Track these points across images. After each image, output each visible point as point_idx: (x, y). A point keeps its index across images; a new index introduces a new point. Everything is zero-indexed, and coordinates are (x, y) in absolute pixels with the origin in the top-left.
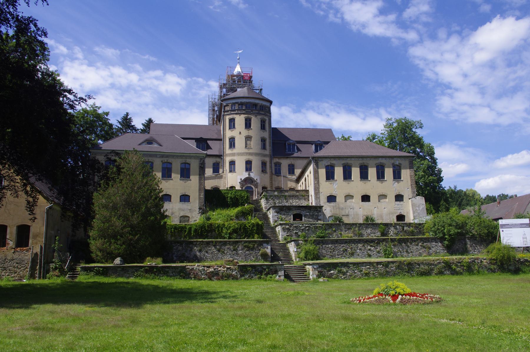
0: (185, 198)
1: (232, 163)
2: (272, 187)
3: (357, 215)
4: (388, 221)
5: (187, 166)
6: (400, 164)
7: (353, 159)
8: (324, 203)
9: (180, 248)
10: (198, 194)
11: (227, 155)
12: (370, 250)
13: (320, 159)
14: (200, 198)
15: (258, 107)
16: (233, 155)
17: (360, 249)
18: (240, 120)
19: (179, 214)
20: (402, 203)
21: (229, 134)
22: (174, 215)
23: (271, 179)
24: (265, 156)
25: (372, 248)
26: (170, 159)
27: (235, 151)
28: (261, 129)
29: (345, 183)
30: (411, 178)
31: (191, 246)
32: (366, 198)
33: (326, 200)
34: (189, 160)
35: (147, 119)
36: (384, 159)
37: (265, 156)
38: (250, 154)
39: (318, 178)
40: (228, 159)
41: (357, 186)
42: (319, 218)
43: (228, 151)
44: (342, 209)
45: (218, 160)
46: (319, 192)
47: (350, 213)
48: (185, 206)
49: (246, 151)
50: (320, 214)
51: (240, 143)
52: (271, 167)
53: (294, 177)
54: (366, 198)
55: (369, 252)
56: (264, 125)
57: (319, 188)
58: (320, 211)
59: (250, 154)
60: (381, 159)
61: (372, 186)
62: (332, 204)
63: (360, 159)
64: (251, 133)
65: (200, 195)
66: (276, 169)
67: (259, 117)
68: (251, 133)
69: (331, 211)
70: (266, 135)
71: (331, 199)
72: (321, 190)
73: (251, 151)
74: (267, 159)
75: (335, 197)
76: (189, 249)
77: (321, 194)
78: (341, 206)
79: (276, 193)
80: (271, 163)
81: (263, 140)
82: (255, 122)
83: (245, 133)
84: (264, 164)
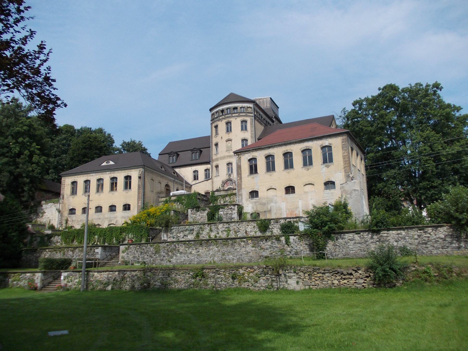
0: (127, 207)
3: (280, 209)
6: (330, 144)
8: (247, 200)
11: (213, 161)
15: (239, 108)
16: (217, 159)
18: (222, 125)
20: (332, 191)
21: (214, 141)
27: (219, 156)
28: (242, 129)
30: (344, 158)
32: (290, 190)
33: (248, 197)
39: (241, 174)
40: (214, 164)
41: (281, 177)
42: (233, 216)
43: (214, 157)
44: (264, 204)
45: (208, 166)
46: (241, 189)
47: (272, 208)
50: (234, 212)
54: (290, 190)
55: (190, 256)
56: (246, 127)
61: (298, 175)
62: (255, 199)
65: (138, 203)
67: (239, 119)
68: (231, 136)
69: (253, 208)
71: (254, 194)
72: (243, 186)
75: (258, 192)
78: (264, 201)
82: (236, 123)
83: (226, 137)
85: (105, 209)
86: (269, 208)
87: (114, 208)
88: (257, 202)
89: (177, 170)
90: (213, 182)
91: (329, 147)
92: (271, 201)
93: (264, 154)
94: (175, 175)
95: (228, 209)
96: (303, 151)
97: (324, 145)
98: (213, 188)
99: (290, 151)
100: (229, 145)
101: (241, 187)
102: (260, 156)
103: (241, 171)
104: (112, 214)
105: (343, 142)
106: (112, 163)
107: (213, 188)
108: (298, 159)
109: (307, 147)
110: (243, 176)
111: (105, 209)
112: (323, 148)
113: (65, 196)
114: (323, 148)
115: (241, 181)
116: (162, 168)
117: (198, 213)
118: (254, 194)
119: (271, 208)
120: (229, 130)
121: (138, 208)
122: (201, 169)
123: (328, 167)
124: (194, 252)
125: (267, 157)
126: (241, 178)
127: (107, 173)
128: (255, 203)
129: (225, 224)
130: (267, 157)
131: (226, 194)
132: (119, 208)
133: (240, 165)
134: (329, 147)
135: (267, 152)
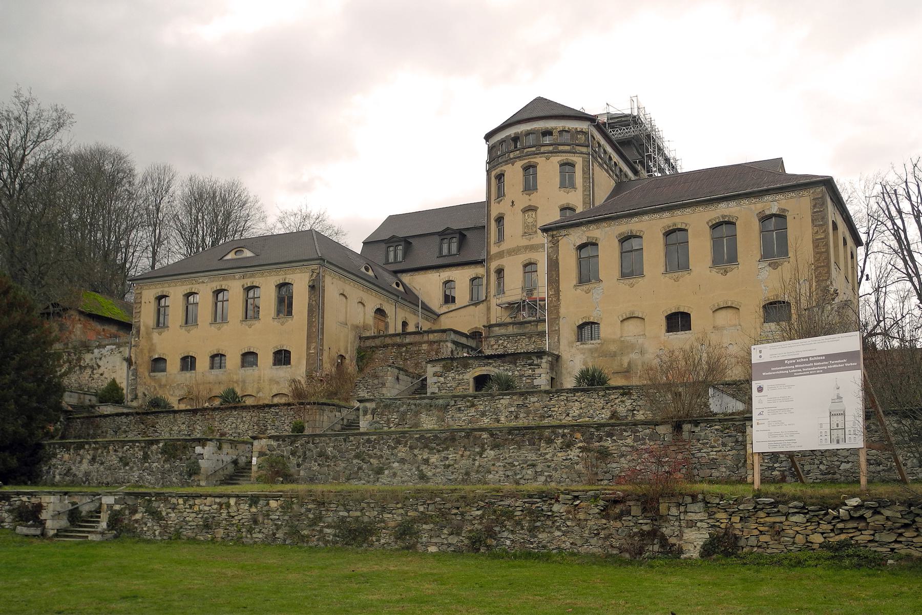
0: (282, 357)
6: (784, 210)
7: (646, 218)
8: (570, 345)
9: (66, 456)
12: (426, 461)
13: (563, 232)
17: (402, 461)
19: (271, 389)
25: (434, 459)
26: (257, 280)
29: (624, 286)
31: (81, 452)
32: (678, 321)
33: (573, 337)
36: (732, 204)
41: (657, 291)
42: (536, 382)
44: (614, 355)
46: (558, 318)
50: (537, 371)
54: (678, 321)
55: (423, 467)
57: (557, 307)
58: (539, 366)
60: (723, 205)
63: (667, 214)
65: (308, 348)
69: (585, 363)
72: (563, 311)
76: (78, 459)
77: (562, 322)
78: (613, 348)
85: (233, 360)
86: (626, 365)
87: (250, 358)
88: (596, 350)
89: (406, 278)
91: (781, 216)
92: (632, 347)
93: (617, 233)
94: (401, 288)
95: (524, 366)
96: (715, 227)
97: (768, 213)
98: (488, 319)
99: (683, 227)
101: (558, 313)
102: (607, 237)
103: (558, 276)
105: (815, 206)
107: (488, 319)
108: (700, 247)
109: (723, 216)
110: (563, 286)
111: (233, 360)
112: (765, 218)
113: (142, 329)
114: (765, 218)
115: (558, 299)
116: (367, 269)
117: (451, 375)
118: (586, 329)
119: (629, 364)
121: (308, 360)
123: (774, 266)
124: (434, 459)
125: (625, 239)
126: (557, 292)
127: (237, 276)
128: (591, 351)
129: (515, 398)
130: (625, 239)
131: (521, 331)
132: (266, 358)
133: (557, 259)
134: (781, 216)
135: (624, 227)
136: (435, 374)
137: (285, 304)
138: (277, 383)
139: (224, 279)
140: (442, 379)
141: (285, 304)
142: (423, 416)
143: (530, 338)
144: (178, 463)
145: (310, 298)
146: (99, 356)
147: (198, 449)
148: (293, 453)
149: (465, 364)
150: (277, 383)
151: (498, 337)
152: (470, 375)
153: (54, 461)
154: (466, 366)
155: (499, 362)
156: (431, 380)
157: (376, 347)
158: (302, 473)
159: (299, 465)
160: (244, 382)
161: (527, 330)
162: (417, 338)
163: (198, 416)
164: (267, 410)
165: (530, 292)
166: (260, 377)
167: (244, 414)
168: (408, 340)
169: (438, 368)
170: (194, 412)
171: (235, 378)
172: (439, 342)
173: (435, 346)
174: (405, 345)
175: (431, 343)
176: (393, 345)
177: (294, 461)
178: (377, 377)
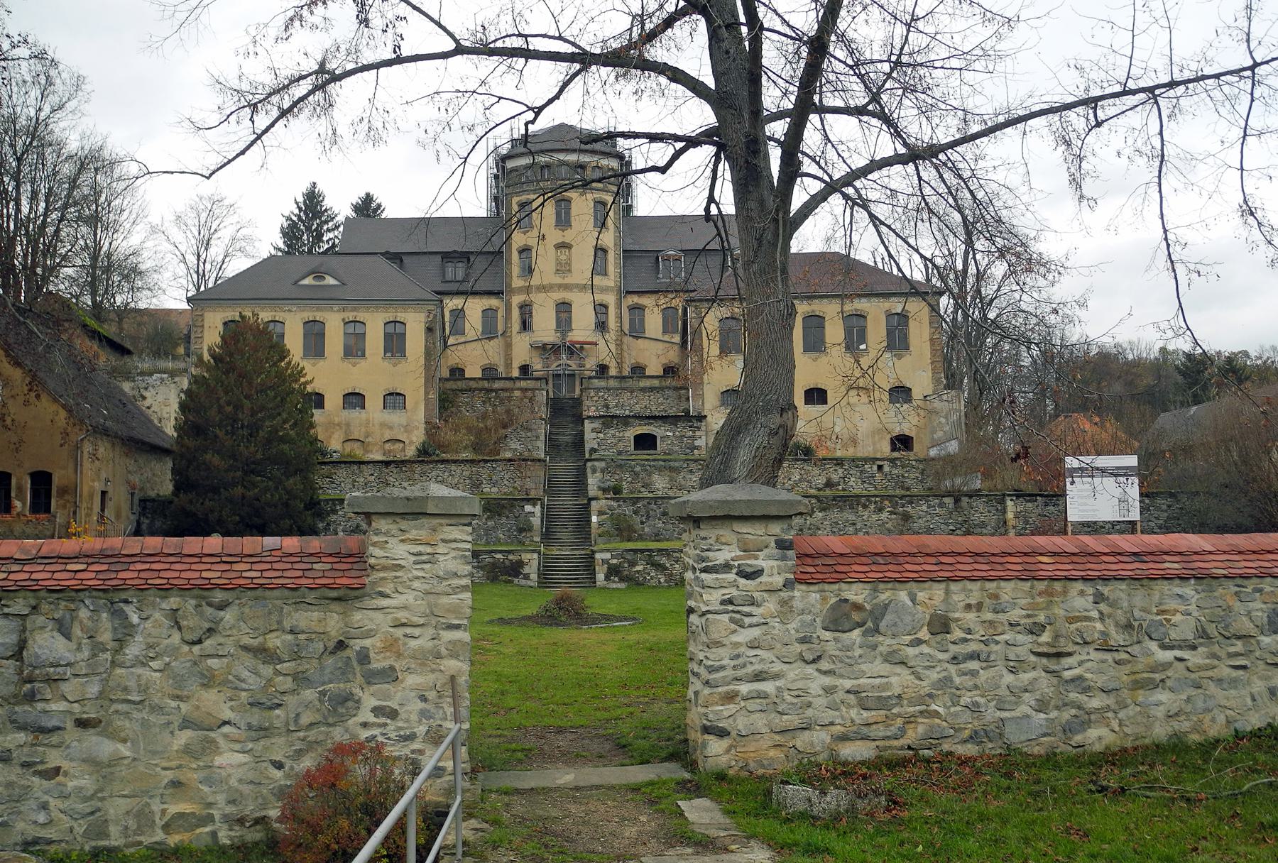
0: (394, 399)
1: (526, 309)
2: (620, 365)
4: (864, 451)
5: (399, 328)
10: (422, 390)
11: (512, 291)
14: (426, 399)
19: (382, 435)
22: (370, 439)
23: (619, 345)
24: (604, 290)
33: (718, 403)
34: (403, 315)
35: (363, 195)
37: (604, 290)
38: (566, 287)
40: (516, 300)
42: (696, 443)
43: (517, 282)
45: (494, 302)
48: (396, 418)
49: (558, 280)
50: (698, 433)
51: (545, 263)
52: (620, 317)
53: (677, 339)
59: (566, 287)
64: (568, 236)
65: (426, 393)
66: (632, 321)
68: (568, 236)
70: (608, 239)
73: (568, 281)
74: (610, 299)
79: (612, 383)
80: (619, 306)
81: (600, 251)
83: (554, 236)
84: (601, 308)
87: (354, 400)
90: (508, 346)
100: (563, 257)
104: (355, 415)
106: (330, 281)
111: (333, 401)
120: (563, 221)
122: (475, 308)
132: (374, 402)
136: (593, 430)
137: (395, 343)
138: (391, 428)
139: (318, 310)
140: (601, 435)
141: (395, 343)
142: (655, 477)
143: (632, 393)
144: (504, 520)
145: (426, 340)
146: (144, 385)
147: (528, 508)
148: (636, 512)
149: (625, 421)
150: (391, 428)
151: (598, 389)
152: (631, 433)
153: (333, 518)
154: (626, 424)
155: (660, 423)
156: (589, 435)
157: (461, 390)
158: (646, 529)
159: (642, 523)
160: (348, 425)
161: (628, 385)
162: (508, 384)
163: (392, 467)
164: (482, 464)
165: (564, 336)
166: (368, 421)
167: (453, 468)
168: (497, 385)
169: (597, 425)
170: (387, 463)
171: (337, 420)
172: (533, 390)
173: (529, 394)
174: (496, 391)
175: (524, 390)
176: (481, 390)
177: (637, 519)
178: (530, 430)
